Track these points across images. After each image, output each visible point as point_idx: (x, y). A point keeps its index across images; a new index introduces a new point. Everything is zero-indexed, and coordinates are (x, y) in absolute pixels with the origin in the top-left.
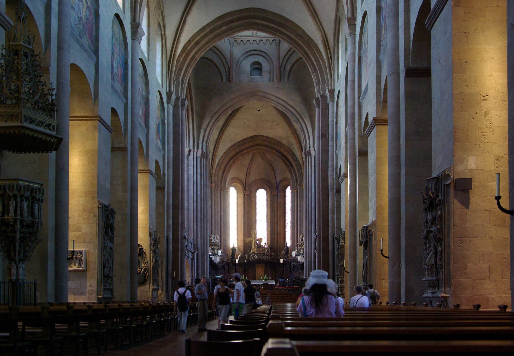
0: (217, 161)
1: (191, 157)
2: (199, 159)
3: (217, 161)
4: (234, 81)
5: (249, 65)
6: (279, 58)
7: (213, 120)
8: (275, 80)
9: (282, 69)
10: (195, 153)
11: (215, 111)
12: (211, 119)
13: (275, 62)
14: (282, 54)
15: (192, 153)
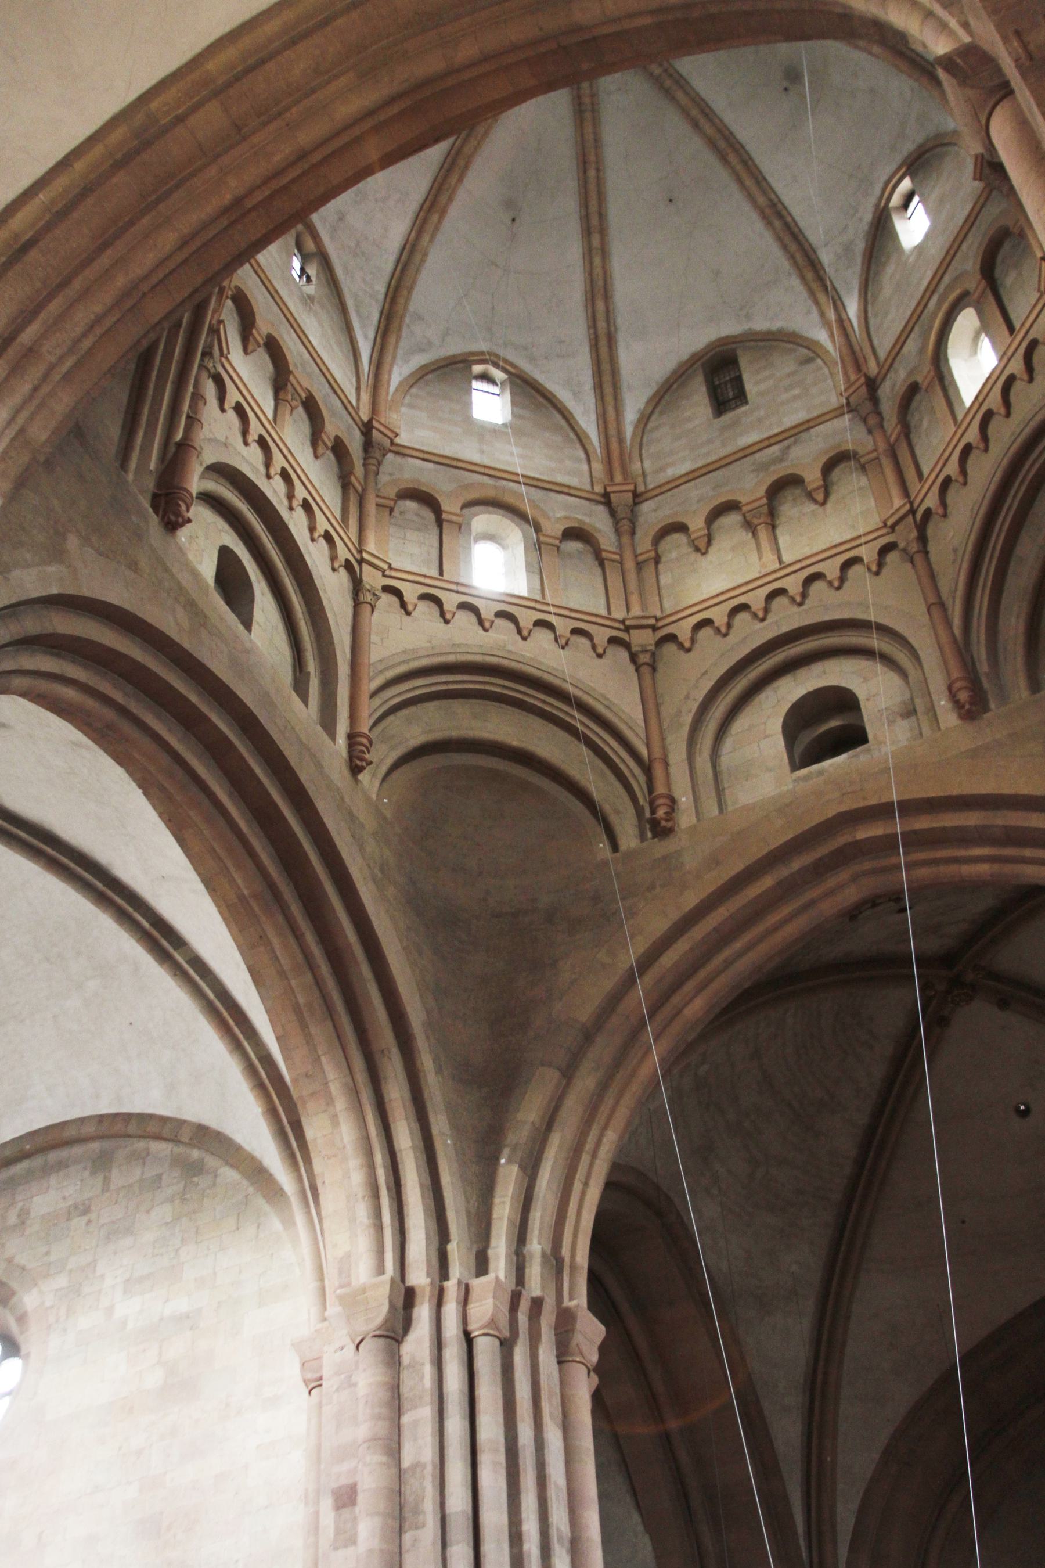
0: (846, 1514)
1: (417, 1343)
2: (486, 1350)
3: (846, 1514)
4: (685, 819)
5: (776, 725)
6: (942, 605)
7: (586, 1082)
8: (949, 718)
9: (981, 653)
10: (451, 1310)
11: (585, 1013)
12: (568, 1073)
13: (923, 639)
14: (952, 577)
15: (423, 1313)
